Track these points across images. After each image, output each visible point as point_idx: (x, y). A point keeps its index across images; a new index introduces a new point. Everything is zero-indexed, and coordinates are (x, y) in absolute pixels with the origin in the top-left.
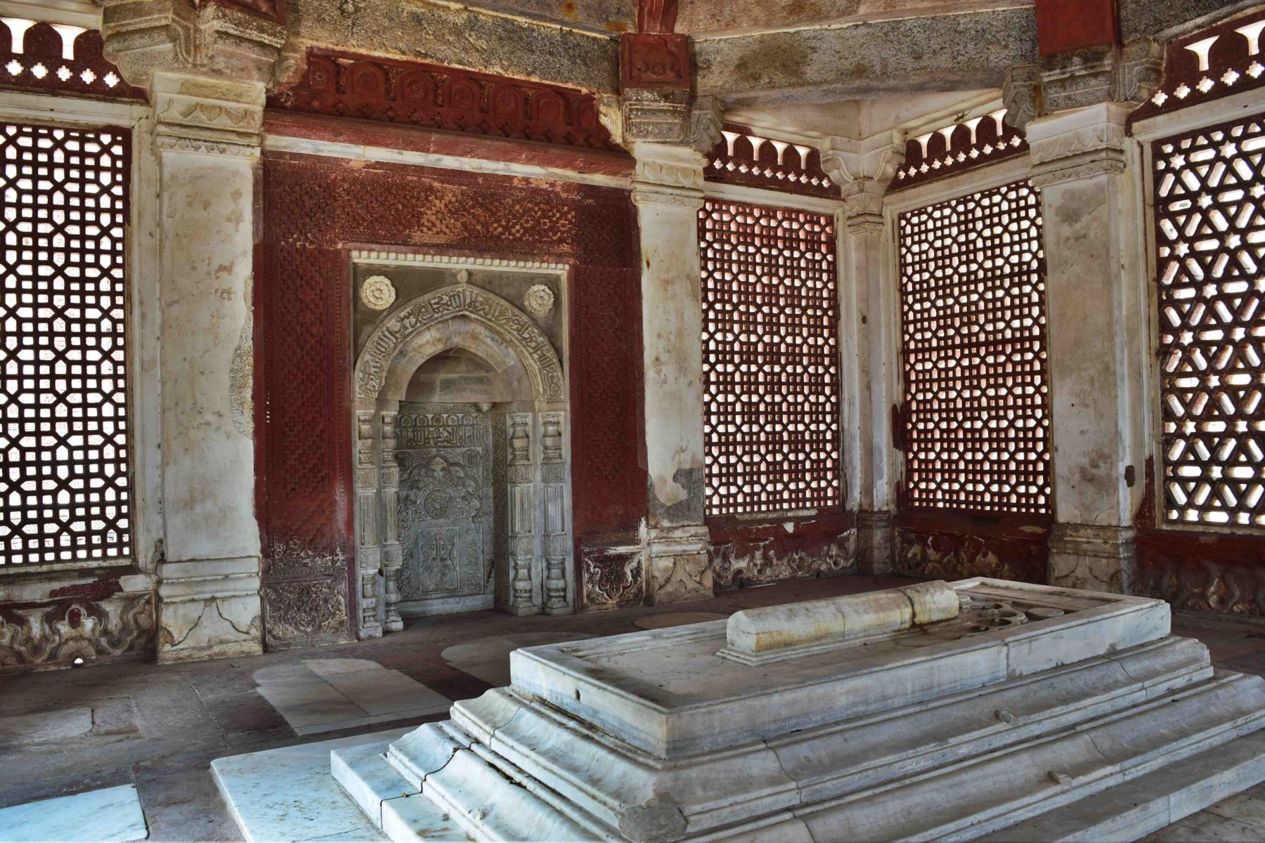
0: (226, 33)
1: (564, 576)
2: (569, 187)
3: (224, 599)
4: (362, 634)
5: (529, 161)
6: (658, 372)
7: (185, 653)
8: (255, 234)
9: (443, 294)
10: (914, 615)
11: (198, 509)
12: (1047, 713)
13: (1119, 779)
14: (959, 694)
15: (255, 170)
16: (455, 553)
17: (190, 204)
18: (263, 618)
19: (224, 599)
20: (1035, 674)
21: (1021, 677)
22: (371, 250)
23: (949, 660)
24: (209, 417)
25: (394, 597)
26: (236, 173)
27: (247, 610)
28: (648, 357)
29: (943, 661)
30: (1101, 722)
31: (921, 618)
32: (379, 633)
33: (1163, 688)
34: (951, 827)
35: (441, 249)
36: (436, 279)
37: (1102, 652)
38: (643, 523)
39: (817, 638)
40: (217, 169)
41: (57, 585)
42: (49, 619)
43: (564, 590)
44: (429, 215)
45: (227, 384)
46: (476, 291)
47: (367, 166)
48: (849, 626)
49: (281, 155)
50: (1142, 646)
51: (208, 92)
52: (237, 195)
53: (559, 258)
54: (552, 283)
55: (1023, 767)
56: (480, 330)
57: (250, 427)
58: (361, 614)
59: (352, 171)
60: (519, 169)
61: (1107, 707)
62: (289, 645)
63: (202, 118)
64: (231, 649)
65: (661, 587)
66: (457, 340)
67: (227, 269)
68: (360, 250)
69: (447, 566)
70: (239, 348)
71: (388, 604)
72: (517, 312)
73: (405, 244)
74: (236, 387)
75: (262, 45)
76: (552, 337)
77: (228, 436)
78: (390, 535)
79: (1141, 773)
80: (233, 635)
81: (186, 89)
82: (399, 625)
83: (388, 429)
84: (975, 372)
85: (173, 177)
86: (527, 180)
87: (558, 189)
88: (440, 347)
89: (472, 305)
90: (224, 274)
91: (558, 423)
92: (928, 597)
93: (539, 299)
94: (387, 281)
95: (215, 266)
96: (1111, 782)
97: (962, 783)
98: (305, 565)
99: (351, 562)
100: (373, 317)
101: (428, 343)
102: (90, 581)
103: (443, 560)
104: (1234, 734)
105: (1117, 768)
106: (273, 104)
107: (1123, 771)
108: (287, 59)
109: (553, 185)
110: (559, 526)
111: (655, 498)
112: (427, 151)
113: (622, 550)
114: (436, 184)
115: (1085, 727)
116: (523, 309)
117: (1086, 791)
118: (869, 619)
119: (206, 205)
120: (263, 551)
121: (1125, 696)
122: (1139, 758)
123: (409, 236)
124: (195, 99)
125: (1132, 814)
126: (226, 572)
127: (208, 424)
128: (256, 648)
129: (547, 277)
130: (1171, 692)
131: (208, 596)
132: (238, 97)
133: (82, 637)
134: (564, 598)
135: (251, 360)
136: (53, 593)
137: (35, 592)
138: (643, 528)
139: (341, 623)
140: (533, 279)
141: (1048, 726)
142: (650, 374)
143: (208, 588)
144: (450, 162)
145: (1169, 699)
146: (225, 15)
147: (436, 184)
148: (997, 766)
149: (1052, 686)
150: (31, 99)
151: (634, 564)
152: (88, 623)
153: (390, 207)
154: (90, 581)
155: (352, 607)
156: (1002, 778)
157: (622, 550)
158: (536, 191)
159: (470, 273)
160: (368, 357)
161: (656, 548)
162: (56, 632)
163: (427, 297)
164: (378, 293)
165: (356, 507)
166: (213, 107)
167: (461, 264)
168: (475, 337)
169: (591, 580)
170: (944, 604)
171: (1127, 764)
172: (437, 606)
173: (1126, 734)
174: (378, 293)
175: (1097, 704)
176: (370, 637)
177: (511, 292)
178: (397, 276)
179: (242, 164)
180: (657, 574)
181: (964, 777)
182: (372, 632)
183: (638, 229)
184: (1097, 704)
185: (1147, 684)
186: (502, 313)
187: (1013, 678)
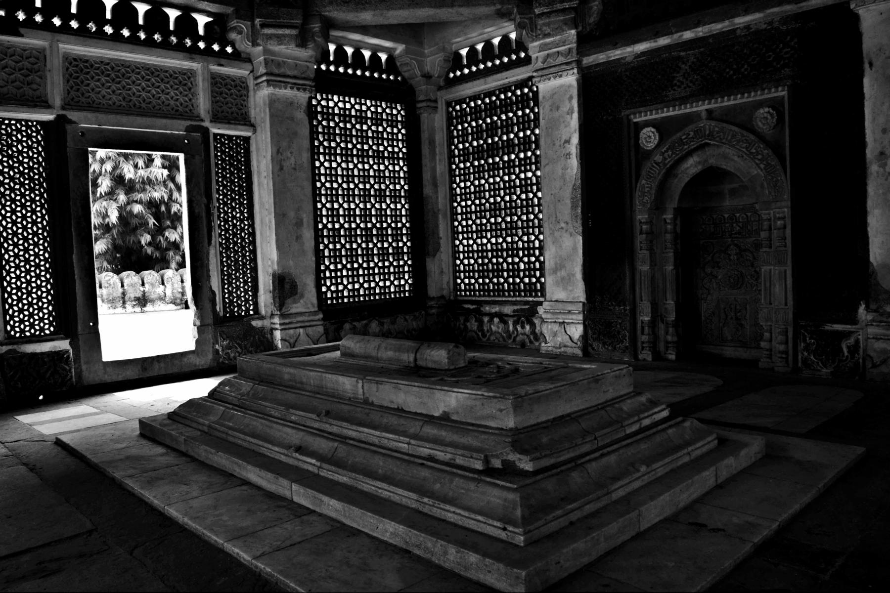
0: (543, 14)
1: (786, 343)
2: (786, 19)
3: (568, 323)
4: (640, 357)
5: (746, 12)
6: (883, 166)
7: (550, 349)
8: (579, 118)
9: (690, 130)
10: (416, 360)
11: (559, 274)
12: (339, 423)
13: (315, 470)
14: (337, 397)
15: (578, 81)
16: (748, 316)
17: (551, 110)
18: (585, 337)
19: (568, 323)
20: (381, 407)
21: (372, 404)
22: (640, 113)
23: (330, 376)
24: (563, 225)
25: (669, 338)
26: (570, 86)
27: (577, 331)
28: (870, 152)
29: (327, 375)
30: (367, 446)
31: (421, 363)
32: (650, 358)
33: (425, 451)
34: (242, 436)
35: (683, 101)
36: (689, 119)
37: (437, 414)
38: (863, 306)
39: (366, 357)
40: (561, 86)
41: (516, 307)
42: (515, 324)
43: (786, 353)
44: (679, 77)
45: (570, 205)
46: (713, 123)
47: (636, 58)
48: (379, 355)
49: (589, 67)
50: (473, 425)
51: (550, 46)
52: (571, 98)
53: (777, 83)
54: (776, 105)
55: (295, 437)
56: (730, 152)
57: (580, 229)
58: (639, 344)
59: (629, 63)
60: (741, 21)
61: (376, 441)
62: (599, 355)
63: (551, 61)
64: (569, 350)
65: (874, 366)
66: (712, 161)
67: (568, 141)
68: (635, 114)
69: (742, 325)
70: (574, 185)
71: (667, 342)
72: (745, 133)
73: (661, 103)
74: (574, 207)
75: (564, 11)
76: (776, 147)
77: (571, 235)
78: (669, 296)
79: (331, 477)
80: (570, 343)
81: (542, 48)
82: (673, 357)
83: (669, 227)
84: (468, 190)
85: (544, 97)
86: (747, 27)
87: (776, 25)
88: (700, 167)
89: (711, 135)
90: (566, 145)
91: (783, 218)
92: (428, 351)
93: (764, 118)
94: (653, 130)
95: (563, 141)
96: (310, 468)
97: (271, 428)
98: (610, 310)
99: (634, 313)
100: (649, 154)
101: (692, 166)
102: (527, 307)
103: (737, 319)
104: (414, 505)
105: (318, 464)
106: (582, 40)
107: (319, 468)
108: (592, 7)
109: (770, 23)
110: (783, 302)
111: (878, 284)
112: (672, 33)
113: (838, 327)
114: (682, 54)
115: (351, 442)
116: (753, 131)
117: (296, 463)
118: (390, 354)
119: (558, 108)
120: (587, 299)
121: (390, 440)
122: (333, 468)
123: (667, 96)
124: (546, 52)
125: (270, 475)
126: (570, 309)
127: (562, 228)
128: (579, 352)
129: (764, 101)
130: (431, 458)
131: (561, 321)
132: (564, 43)
133: (524, 334)
134: (787, 359)
135: (580, 191)
136: (514, 311)
137: (508, 310)
138: (862, 310)
139: (627, 347)
140: (760, 104)
141: (335, 429)
142: (874, 168)
143: (560, 316)
144: (688, 35)
145: (420, 461)
146: (540, 4)
147: (682, 54)
148: (289, 430)
149: (368, 414)
150: (505, 74)
151: (852, 341)
152: (528, 327)
153: (651, 80)
154: (527, 307)
155: (634, 339)
156: (285, 436)
157: (838, 327)
158: (758, 32)
159: (709, 112)
160: (644, 182)
161: (871, 330)
162: (516, 329)
163: (678, 135)
164: (649, 138)
165: (637, 277)
166: (555, 53)
167: (702, 107)
168: (725, 157)
169: (807, 348)
170: (436, 358)
171: (325, 466)
172: (729, 352)
173: (359, 457)
174: (649, 138)
175: (351, 431)
176: (644, 360)
177: (740, 119)
178: (655, 124)
179: (570, 79)
180: (872, 354)
181: (275, 425)
182: (645, 356)
183: (859, 35)
184: (351, 431)
185: (412, 442)
186: (734, 136)
187: (366, 402)
